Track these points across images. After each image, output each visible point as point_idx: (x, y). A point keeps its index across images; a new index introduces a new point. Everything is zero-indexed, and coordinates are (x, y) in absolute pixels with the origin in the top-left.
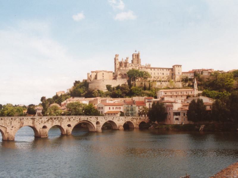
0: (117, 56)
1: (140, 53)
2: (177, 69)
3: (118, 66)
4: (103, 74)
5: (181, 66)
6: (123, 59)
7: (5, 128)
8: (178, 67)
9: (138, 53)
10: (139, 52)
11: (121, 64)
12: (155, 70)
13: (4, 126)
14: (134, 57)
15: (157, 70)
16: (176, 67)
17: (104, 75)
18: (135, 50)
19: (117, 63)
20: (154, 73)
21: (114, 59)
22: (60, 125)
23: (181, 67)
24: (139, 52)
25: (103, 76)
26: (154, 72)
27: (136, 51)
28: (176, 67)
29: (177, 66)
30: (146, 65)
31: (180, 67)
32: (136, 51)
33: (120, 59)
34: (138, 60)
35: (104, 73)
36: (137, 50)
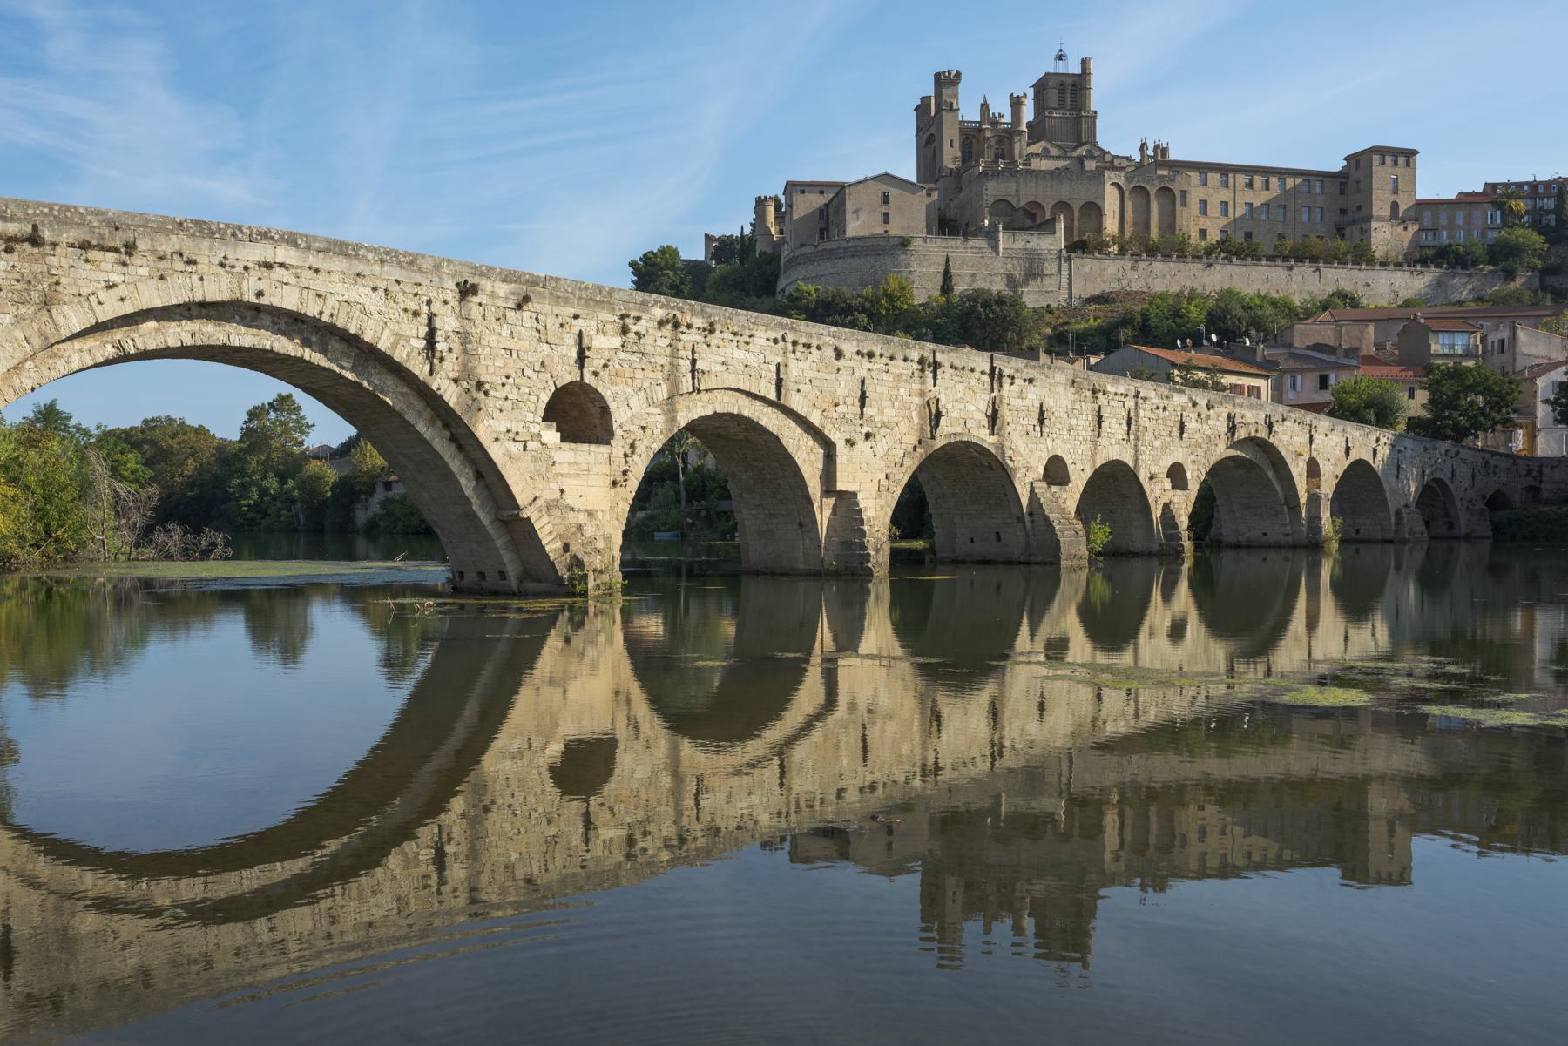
0: (946, 82)
1: (1093, 67)
2: (1382, 175)
3: (950, 156)
4: (886, 199)
5: (1410, 154)
6: (985, 106)
7: (820, 452)
8: (1389, 159)
9: (1078, 71)
10: (1085, 63)
11: (971, 137)
12: (1231, 176)
13: (815, 419)
14: (1052, 98)
15: (1242, 179)
16: (1376, 159)
17: (892, 209)
18: (1055, 52)
19: (950, 133)
20: (1226, 204)
21: (922, 109)
22: (1131, 464)
23: (1408, 165)
24: (1085, 63)
25: (886, 215)
26: (1225, 195)
27: (1060, 57)
28: (1376, 159)
29: (1382, 151)
30: (1142, 149)
31: (1401, 160)
32: (1060, 57)
33: (969, 112)
34: (1078, 119)
35: (894, 193)
36: (1066, 50)
